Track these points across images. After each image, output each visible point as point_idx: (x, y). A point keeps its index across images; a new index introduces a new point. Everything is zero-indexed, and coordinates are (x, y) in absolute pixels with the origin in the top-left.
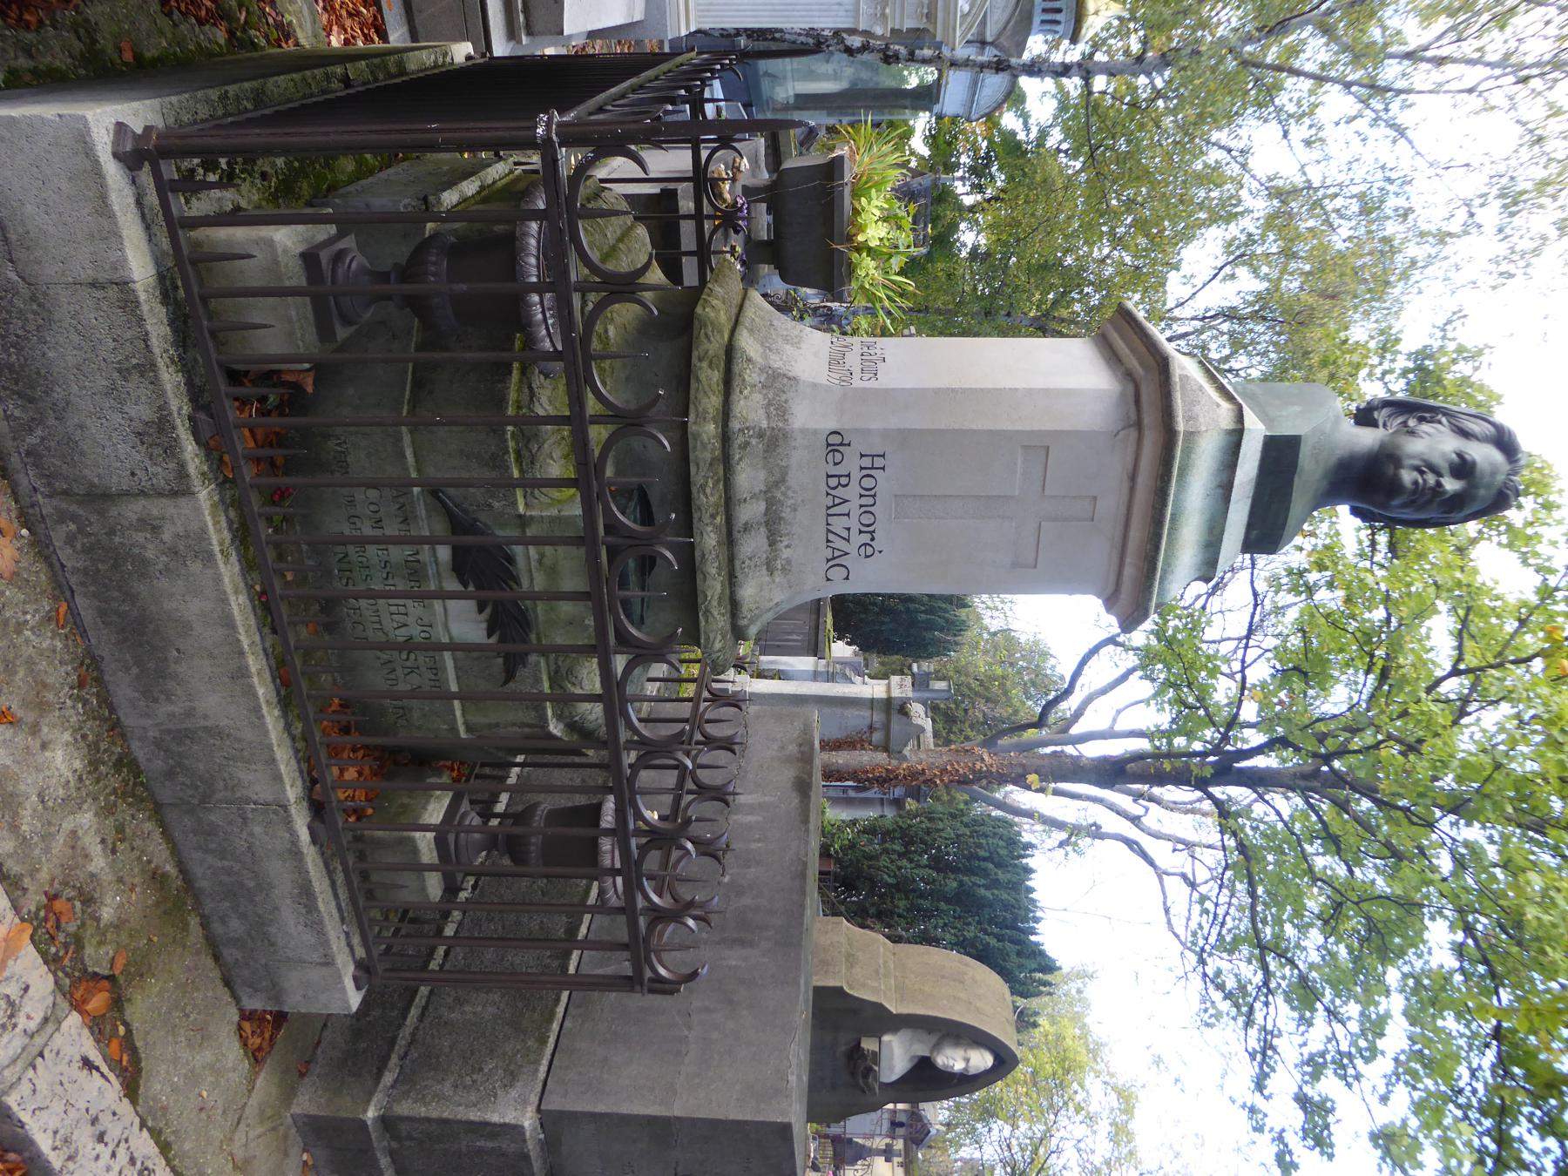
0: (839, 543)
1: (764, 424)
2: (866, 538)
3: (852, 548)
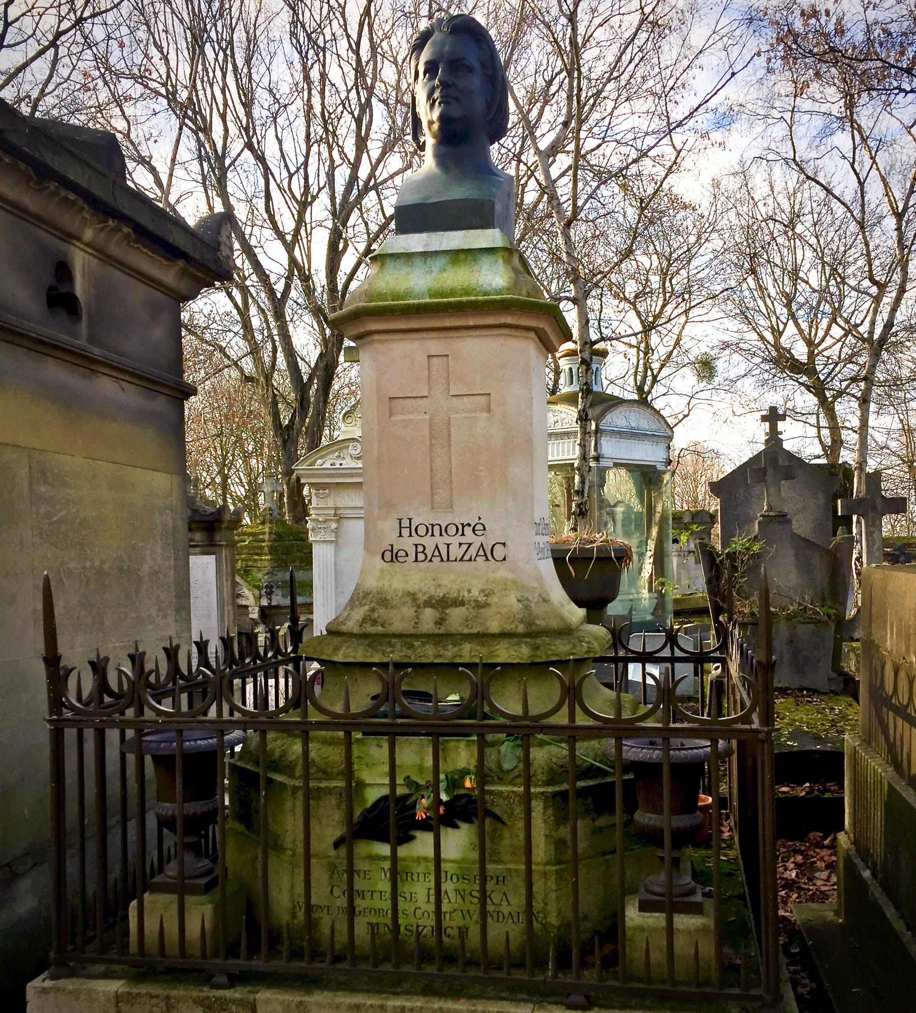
0: (473, 551)
1: (367, 607)
2: (468, 531)
3: (477, 541)
